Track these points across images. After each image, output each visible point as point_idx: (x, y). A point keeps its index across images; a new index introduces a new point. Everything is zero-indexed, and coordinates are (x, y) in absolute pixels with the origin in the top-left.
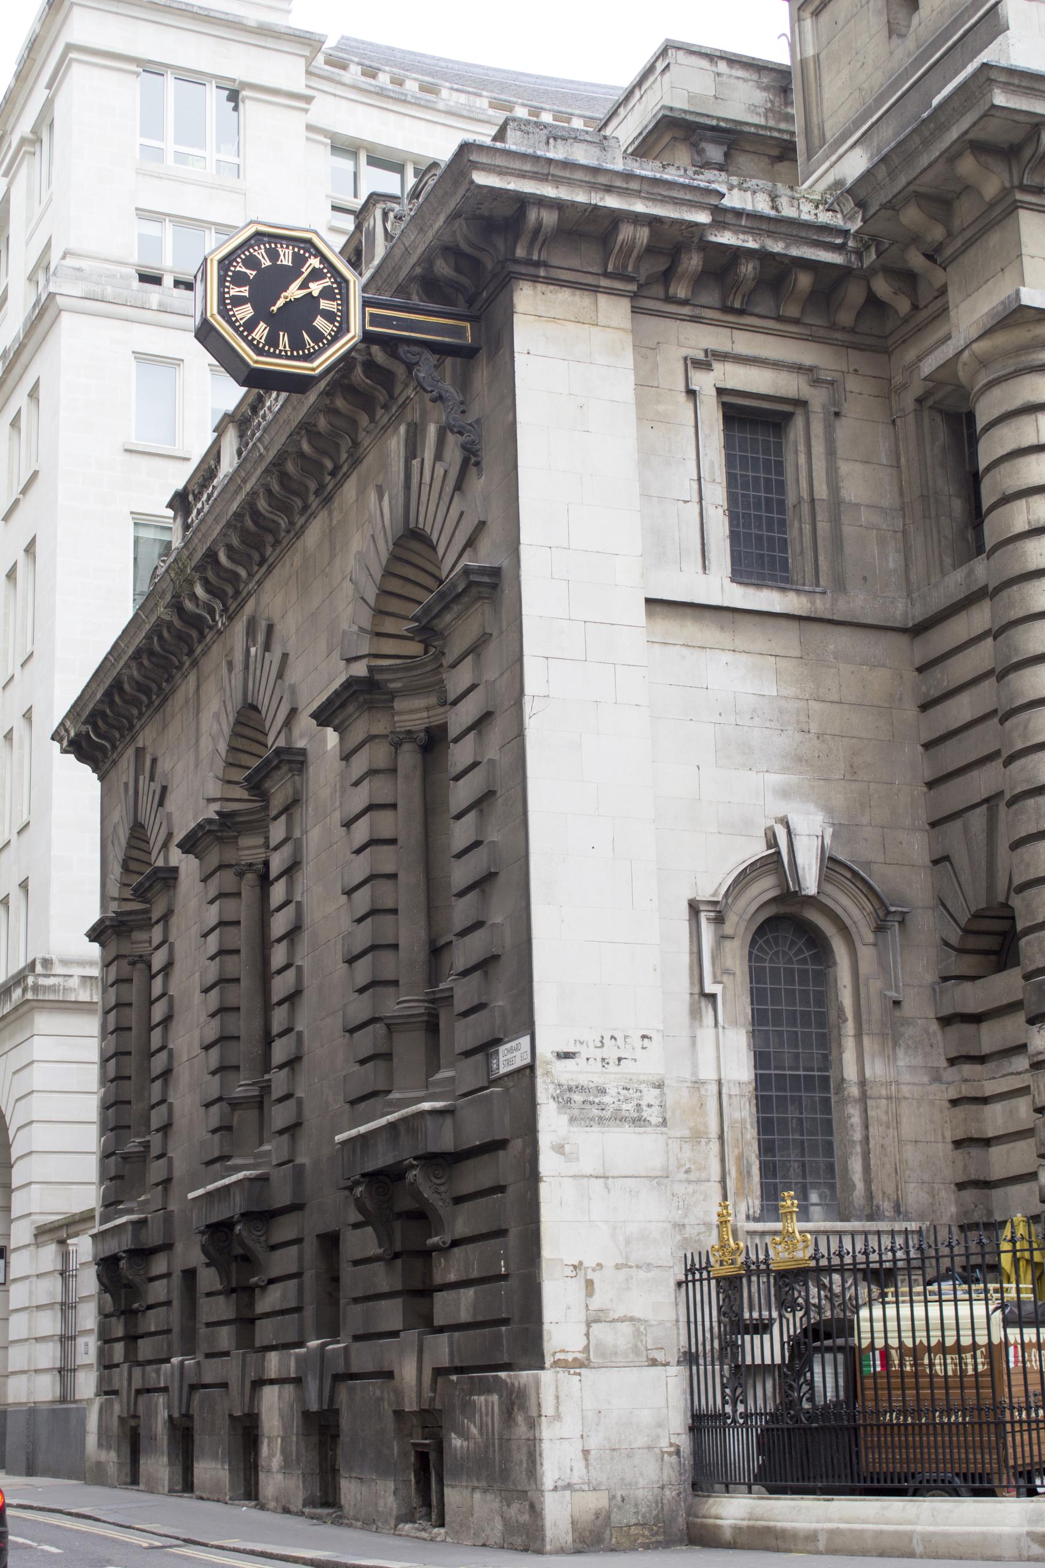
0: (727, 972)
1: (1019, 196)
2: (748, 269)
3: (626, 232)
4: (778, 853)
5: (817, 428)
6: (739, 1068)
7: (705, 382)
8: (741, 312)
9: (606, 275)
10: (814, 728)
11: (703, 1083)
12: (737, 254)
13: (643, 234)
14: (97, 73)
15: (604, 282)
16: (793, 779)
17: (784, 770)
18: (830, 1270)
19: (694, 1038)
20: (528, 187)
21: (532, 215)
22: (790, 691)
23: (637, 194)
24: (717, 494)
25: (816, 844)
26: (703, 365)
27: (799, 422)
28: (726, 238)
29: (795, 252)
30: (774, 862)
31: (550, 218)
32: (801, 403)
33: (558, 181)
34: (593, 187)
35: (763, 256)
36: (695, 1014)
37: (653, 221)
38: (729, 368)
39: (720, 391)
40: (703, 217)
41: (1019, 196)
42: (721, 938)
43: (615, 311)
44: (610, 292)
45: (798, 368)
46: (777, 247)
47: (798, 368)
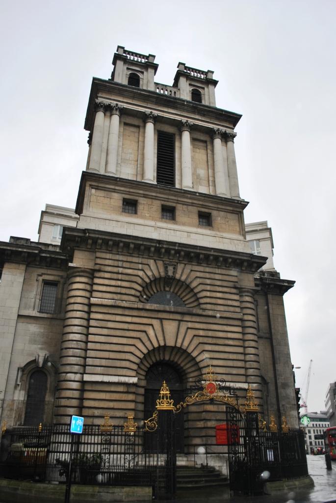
0: (23, 380)
1: (75, 248)
2: (48, 260)
3: (23, 254)
4: (36, 360)
5: (61, 286)
6: (22, 398)
7: (41, 278)
8: (49, 267)
9: (22, 261)
10: (50, 337)
11: (15, 400)
12: (46, 257)
13: (26, 255)
15: (21, 262)
16: (43, 346)
17: (42, 345)
18: (29, 436)
19: (14, 393)
20: (5, 248)
21: (6, 252)
22: (46, 331)
23: (25, 248)
24: (38, 297)
25: (43, 358)
26: (41, 276)
27: (58, 285)
28: (43, 255)
29: (56, 257)
30: (34, 361)
32: (59, 282)
33: (10, 247)
34: (17, 247)
35: (50, 257)
36: (15, 388)
37: (29, 253)
38: (46, 276)
39: (43, 280)
40: (37, 252)
41: (75, 248)
42: (23, 375)
43: (23, 267)
44: (22, 264)
45: (59, 276)
46: (53, 256)
47: (59, 276)
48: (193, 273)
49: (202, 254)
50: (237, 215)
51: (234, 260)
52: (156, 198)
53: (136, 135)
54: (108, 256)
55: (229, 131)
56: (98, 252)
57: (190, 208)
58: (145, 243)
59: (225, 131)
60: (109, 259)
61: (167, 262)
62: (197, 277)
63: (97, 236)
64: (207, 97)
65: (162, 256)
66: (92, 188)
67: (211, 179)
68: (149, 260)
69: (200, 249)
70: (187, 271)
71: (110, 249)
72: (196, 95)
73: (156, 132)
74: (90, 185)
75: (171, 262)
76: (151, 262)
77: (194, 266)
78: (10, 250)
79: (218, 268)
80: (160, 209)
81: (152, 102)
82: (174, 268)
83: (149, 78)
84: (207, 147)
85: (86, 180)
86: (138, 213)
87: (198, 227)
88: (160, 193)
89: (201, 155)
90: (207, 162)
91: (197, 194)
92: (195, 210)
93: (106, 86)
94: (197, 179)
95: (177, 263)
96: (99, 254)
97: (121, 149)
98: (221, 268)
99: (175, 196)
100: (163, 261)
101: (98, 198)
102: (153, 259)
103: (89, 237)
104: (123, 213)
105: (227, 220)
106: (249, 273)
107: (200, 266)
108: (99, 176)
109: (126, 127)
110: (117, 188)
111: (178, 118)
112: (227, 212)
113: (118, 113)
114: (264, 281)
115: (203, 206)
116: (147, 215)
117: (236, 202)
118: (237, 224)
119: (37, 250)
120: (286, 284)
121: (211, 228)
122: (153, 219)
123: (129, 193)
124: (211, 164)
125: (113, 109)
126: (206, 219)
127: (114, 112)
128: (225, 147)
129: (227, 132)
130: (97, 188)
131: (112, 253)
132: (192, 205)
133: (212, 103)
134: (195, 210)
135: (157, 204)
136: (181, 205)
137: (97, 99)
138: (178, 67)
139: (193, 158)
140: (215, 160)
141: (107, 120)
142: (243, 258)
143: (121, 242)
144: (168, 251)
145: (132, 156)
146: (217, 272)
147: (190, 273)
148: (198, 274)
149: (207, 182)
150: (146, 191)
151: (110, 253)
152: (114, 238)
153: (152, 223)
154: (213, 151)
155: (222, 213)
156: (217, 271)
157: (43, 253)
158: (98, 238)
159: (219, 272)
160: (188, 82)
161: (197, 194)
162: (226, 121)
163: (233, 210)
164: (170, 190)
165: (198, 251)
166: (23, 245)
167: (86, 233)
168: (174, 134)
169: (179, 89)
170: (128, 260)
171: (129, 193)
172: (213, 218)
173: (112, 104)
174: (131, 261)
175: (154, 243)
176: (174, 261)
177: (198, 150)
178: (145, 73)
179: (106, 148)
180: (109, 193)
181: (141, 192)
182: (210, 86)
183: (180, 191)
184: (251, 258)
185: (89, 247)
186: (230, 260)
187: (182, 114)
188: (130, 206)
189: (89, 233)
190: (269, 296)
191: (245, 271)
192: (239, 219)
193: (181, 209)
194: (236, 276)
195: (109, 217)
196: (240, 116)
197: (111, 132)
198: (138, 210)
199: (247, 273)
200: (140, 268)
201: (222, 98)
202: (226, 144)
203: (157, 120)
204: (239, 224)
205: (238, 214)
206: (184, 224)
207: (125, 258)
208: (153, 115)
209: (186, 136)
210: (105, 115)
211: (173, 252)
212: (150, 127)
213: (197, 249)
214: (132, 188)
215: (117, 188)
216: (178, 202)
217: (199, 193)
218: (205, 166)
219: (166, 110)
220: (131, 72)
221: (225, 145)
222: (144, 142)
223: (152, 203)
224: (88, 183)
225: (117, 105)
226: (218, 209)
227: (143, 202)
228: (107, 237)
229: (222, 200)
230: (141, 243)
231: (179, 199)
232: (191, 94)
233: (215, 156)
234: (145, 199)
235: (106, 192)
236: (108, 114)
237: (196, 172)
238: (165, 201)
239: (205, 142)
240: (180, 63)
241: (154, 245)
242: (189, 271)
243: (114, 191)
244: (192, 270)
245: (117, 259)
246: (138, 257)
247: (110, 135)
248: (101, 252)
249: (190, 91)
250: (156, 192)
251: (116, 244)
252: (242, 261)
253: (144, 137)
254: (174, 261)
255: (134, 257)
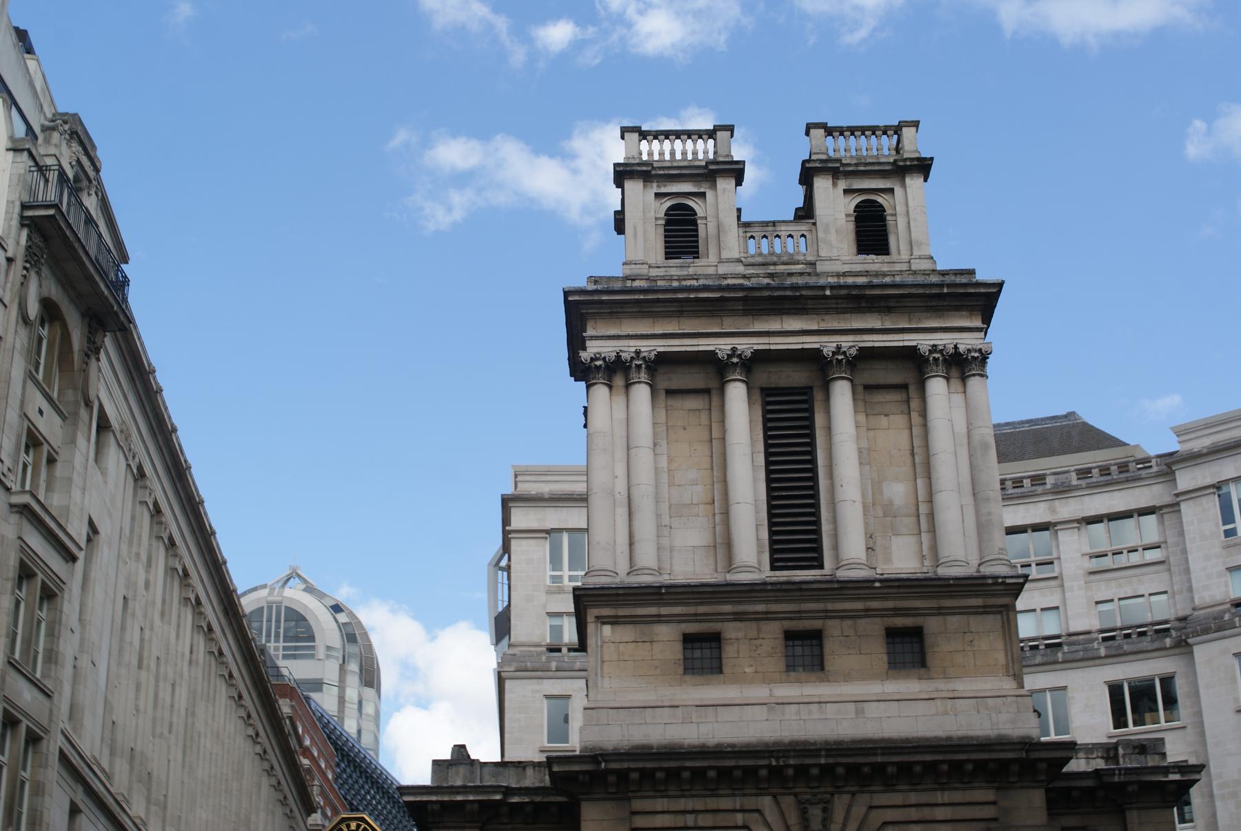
3: (469, 807)
13: (476, 806)
14: (524, 542)
20: (425, 798)
21: (429, 807)
23: (470, 793)
28: (515, 800)
29: (546, 800)
31: (437, 807)
33: (436, 794)
40: (498, 797)
46: (538, 799)
48: (874, 813)
49: (892, 763)
50: (998, 617)
51: (981, 766)
52: (767, 617)
53: (704, 416)
54: (660, 804)
55: (966, 342)
56: (636, 798)
57: (863, 622)
58: (742, 763)
59: (956, 347)
60: (663, 812)
61: (808, 797)
62: (885, 823)
63: (625, 765)
64: (901, 222)
65: (791, 785)
66: (604, 623)
67: (923, 509)
68: (760, 798)
69: (883, 754)
70: (859, 810)
71: (662, 788)
72: (872, 230)
73: (757, 396)
74: (597, 617)
75: (815, 795)
76: (766, 802)
77: (875, 796)
78: (437, 802)
79: (943, 790)
80: (779, 643)
81: (733, 313)
82: (825, 810)
83: (721, 215)
84: (908, 401)
85: (586, 608)
86: (725, 670)
87: (887, 677)
88: (776, 601)
89: (893, 432)
90: (913, 454)
91: (877, 584)
92: (875, 627)
93: (602, 302)
94: (885, 516)
95: (832, 795)
96: (638, 805)
97: (665, 478)
98: (949, 789)
99: (817, 601)
100: (796, 795)
101: (622, 647)
102: (769, 794)
103: (608, 771)
104: (687, 678)
105: (968, 637)
106: (1033, 787)
107: (894, 791)
108: (614, 592)
109: (670, 402)
110: (664, 611)
111: (811, 342)
112: (968, 613)
113: (643, 376)
114: (1106, 779)
115: (897, 612)
116: (747, 670)
117: (990, 581)
118: (1000, 645)
119: (497, 793)
120: (1177, 777)
121: (922, 671)
122: (767, 680)
123: (696, 618)
124: (922, 463)
125: (630, 367)
126: (908, 649)
127: (634, 376)
128: (958, 399)
129: (962, 348)
130: (615, 621)
131: (668, 797)
132: (868, 613)
133: (920, 244)
134: (875, 627)
135: (773, 630)
136: (837, 622)
137: (584, 349)
138: (807, 134)
139: (865, 457)
140: (933, 450)
141: (620, 400)
142: (1002, 755)
143: (686, 768)
144: (802, 771)
145: (699, 489)
146: (940, 801)
147: (866, 815)
148: (890, 815)
149: (914, 519)
150: (739, 603)
151: (662, 797)
152: (666, 764)
153: (760, 692)
154: (924, 413)
155: (954, 621)
156: (940, 797)
157: (514, 795)
158: (629, 770)
159: (946, 800)
160: (842, 184)
161: (877, 584)
162: (958, 308)
163: (984, 607)
164: (801, 590)
165: (879, 759)
166: (464, 787)
167: (600, 763)
168: (811, 388)
169: (814, 224)
170: (709, 807)
171: (696, 618)
172: (928, 641)
173: (625, 356)
174: (715, 807)
175: (764, 758)
176: (822, 789)
177: (884, 421)
178: (709, 194)
179: (625, 493)
180: (646, 627)
181: (727, 608)
182: (908, 180)
183: (829, 586)
184: (1027, 751)
185: (610, 790)
186: (970, 767)
187: (824, 326)
188: (703, 653)
189: (605, 761)
190: (1128, 814)
191: (1019, 784)
192: (1003, 626)
193: (837, 632)
194: (994, 803)
195: (650, 697)
196: (1000, 285)
197: (632, 445)
198: (724, 661)
199: (1022, 788)
200: (740, 823)
201: (936, 231)
202: (965, 385)
203: (752, 364)
204: (1006, 645)
205: (1000, 612)
206: (848, 677)
207: (698, 804)
208: (739, 356)
209: (842, 394)
210: (610, 387)
211: (815, 771)
212: (737, 394)
213: (875, 755)
214: (702, 604)
215: (664, 611)
216: (828, 615)
217: (880, 581)
218: (906, 469)
219: (774, 325)
220: (669, 204)
221: (960, 388)
222: (723, 439)
223: (759, 630)
224: (592, 614)
225: (638, 353)
226: (941, 612)
227: (733, 636)
228: (648, 765)
229: (950, 585)
230: (731, 763)
231: (830, 606)
232: (851, 227)
233: (931, 437)
234: (738, 624)
235: (638, 627)
236: (619, 381)
237: (882, 493)
238: (791, 619)
239: (904, 387)
240: (809, 128)
241: (765, 762)
242: (864, 809)
243: (659, 619)
244: (871, 807)
245: (682, 808)
246: (733, 795)
247: (633, 452)
248: (642, 797)
249: (847, 215)
250: (766, 602)
251: (673, 775)
252: (1004, 765)
253: (723, 421)
254: (822, 789)
255: (722, 796)
